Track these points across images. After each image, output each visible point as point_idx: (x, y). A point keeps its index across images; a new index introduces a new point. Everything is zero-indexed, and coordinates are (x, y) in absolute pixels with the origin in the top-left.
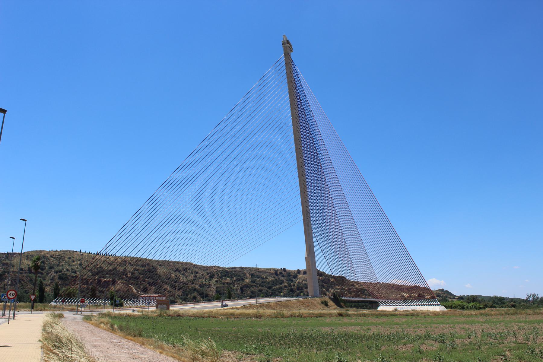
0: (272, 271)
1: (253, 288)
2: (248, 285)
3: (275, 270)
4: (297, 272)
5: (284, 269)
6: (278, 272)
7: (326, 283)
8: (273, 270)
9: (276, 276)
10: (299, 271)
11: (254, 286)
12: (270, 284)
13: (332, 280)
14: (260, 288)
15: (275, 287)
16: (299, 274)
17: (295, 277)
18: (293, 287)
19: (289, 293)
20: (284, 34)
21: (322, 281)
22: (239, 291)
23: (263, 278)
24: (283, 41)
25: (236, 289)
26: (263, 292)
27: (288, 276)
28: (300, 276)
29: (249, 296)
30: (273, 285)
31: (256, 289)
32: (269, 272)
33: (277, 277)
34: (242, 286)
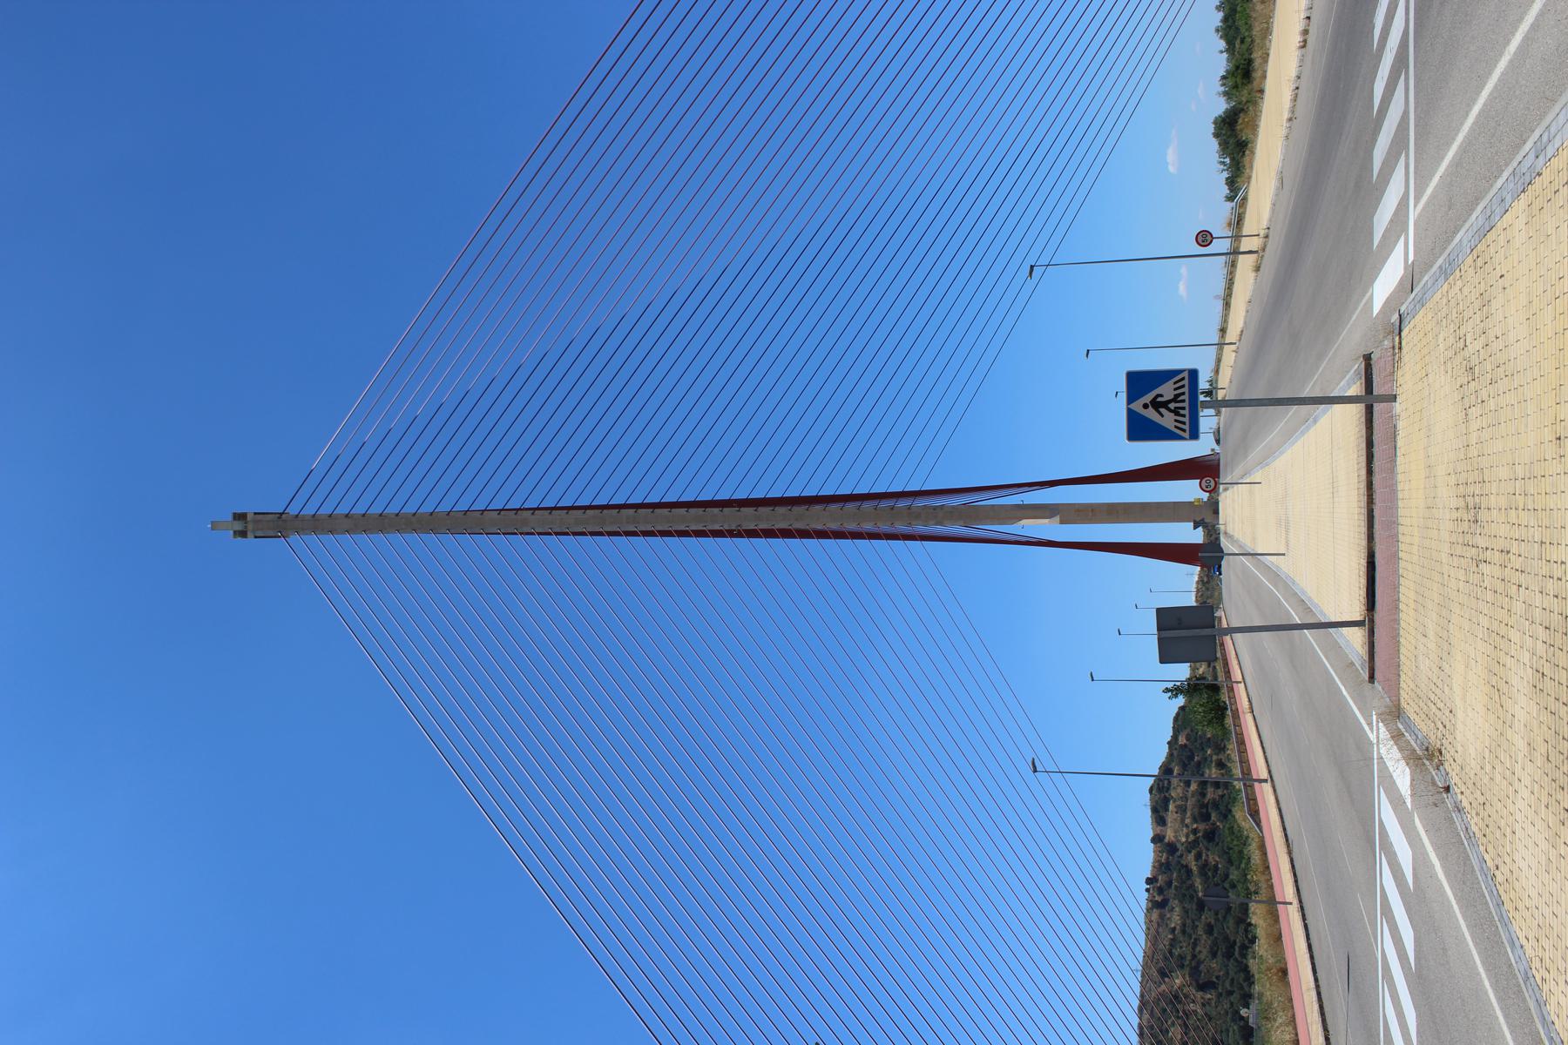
0: (1155, 916)
1: (1200, 952)
2: (1191, 968)
3: (1152, 909)
4: (1159, 845)
5: (1149, 881)
6: (1159, 898)
7: (1193, 754)
8: (1151, 916)
9: (1170, 904)
10: (1157, 839)
11: (1194, 949)
12: (1189, 907)
13: (1182, 740)
14: (1200, 931)
15: (1200, 887)
16: (1164, 837)
17: (1171, 848)
18: (1200, 834)
19: (1218, 844)
20: (210, 526)
21: (1184, 767)
22: (1209, 996)
23: (1171, 939)
24: (235, 532)
25: (1203, 1005)
26: (1213, 922)
27: (1170, 869)
28: (1170, 835)
29: (1225, 960)
30: (1192, 897)
31: (1203, 942)
32: (1155, 925)
33: (1174, 903)
34: (1194, 983)
